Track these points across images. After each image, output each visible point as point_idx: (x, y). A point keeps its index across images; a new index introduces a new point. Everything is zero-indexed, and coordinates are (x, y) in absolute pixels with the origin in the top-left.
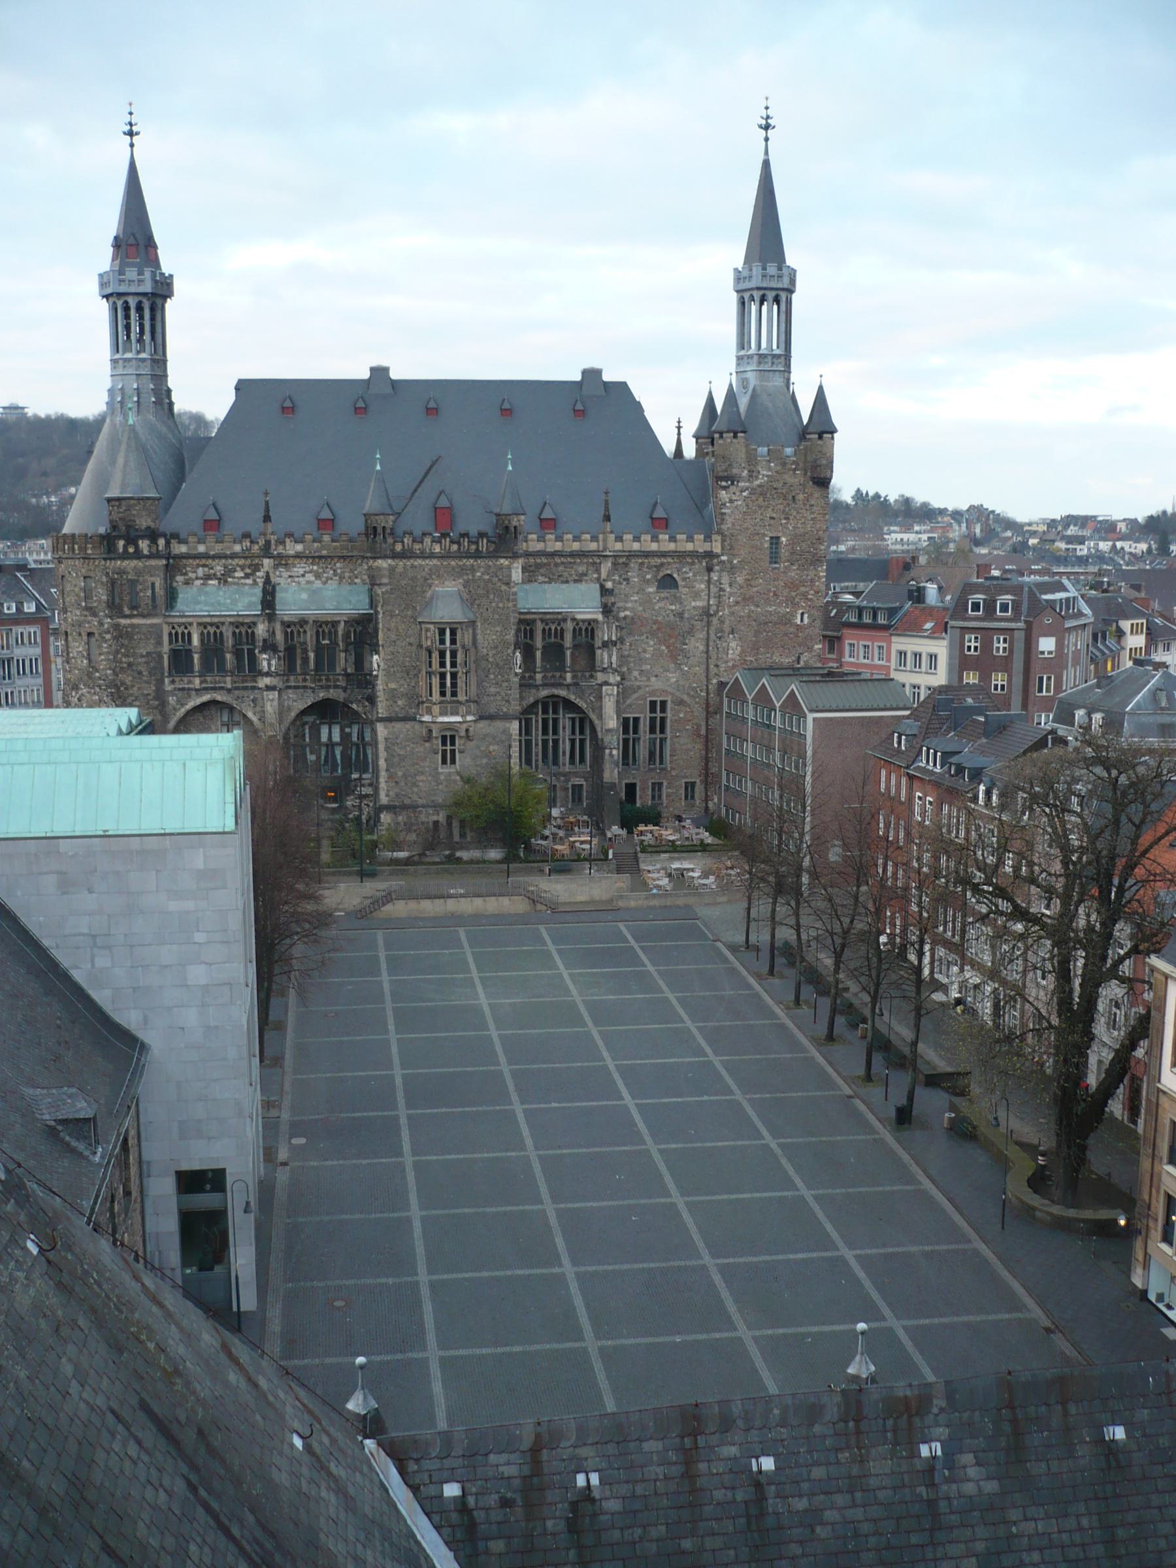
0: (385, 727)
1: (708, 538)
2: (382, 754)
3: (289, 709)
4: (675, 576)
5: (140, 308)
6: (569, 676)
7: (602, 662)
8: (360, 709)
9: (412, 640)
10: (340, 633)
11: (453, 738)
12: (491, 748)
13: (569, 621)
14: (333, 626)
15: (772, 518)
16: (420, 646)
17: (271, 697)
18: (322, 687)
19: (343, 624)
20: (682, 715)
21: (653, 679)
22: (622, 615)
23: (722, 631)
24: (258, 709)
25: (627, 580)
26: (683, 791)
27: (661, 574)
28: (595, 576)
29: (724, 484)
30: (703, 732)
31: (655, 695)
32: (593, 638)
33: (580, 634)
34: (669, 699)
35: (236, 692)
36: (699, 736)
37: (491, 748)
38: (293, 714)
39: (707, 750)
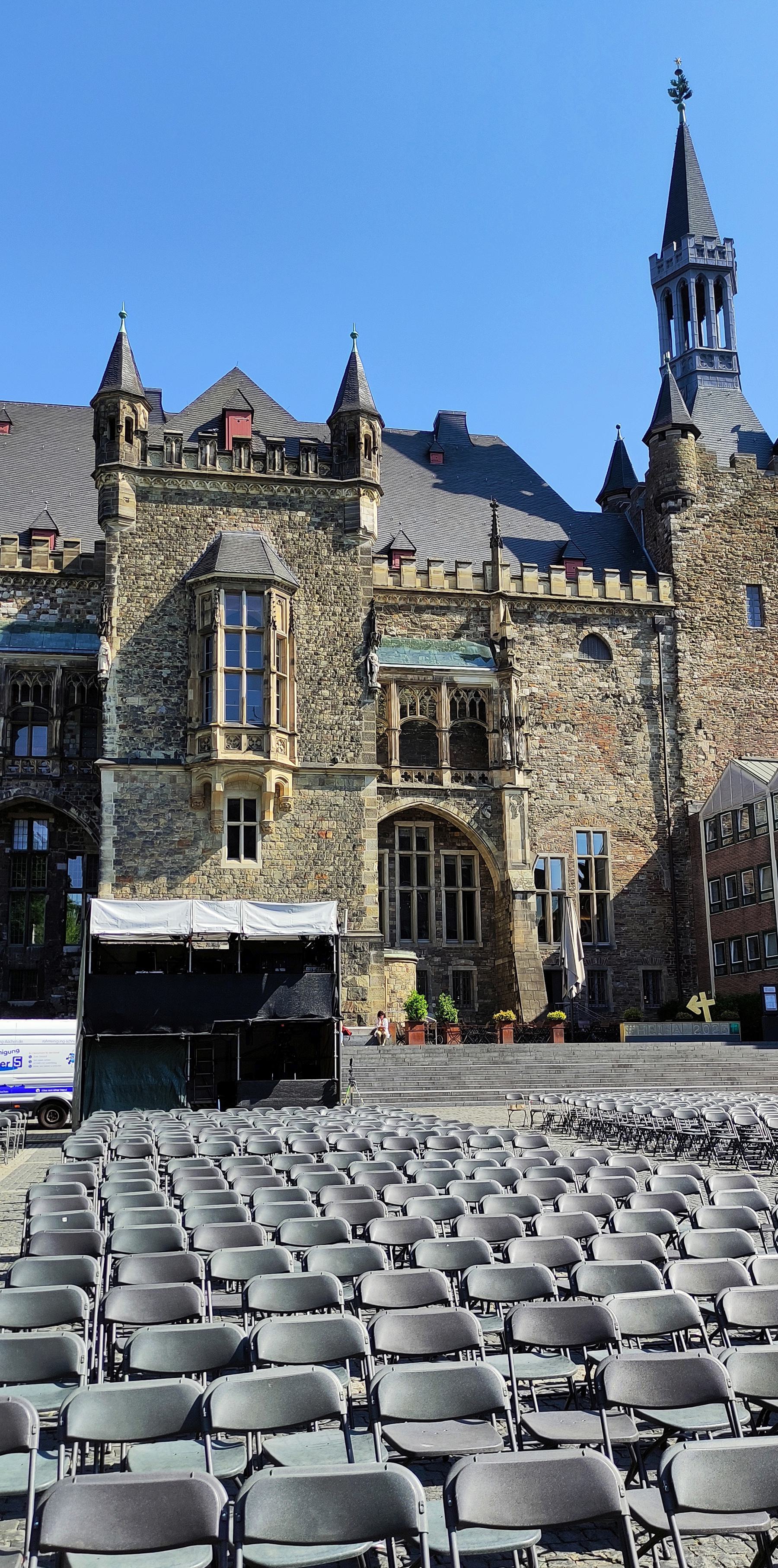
0: (118, 778)
1: (653, 581)
2: (109, 832)
4: (606, 636)
6: (447, 776)
7: (501, 752)
8: (83, 817)
9: (176, 621)
10: (54, 688)
11: (251, 805)
12: (325, 825)
13: (444, 687)
14: (43, 677)
15: (746, 558)
16: (192, 628)
18: (16, 777)
19: (59, 673)
20: (629, 858)
21: (581, 797)
22: (527, 692)
23: (685, 723)
25: (531, 638)
26: (640, 987)
27: (585, 633)
28: (482, 629)
29: (671, 504)
30: (666, 886)
31: (583, 824)
32: (483, 718)
33: (462, 711)
34: (608, 828)
36: (660, 892)
37: (325, 825)
39: (677, 918)
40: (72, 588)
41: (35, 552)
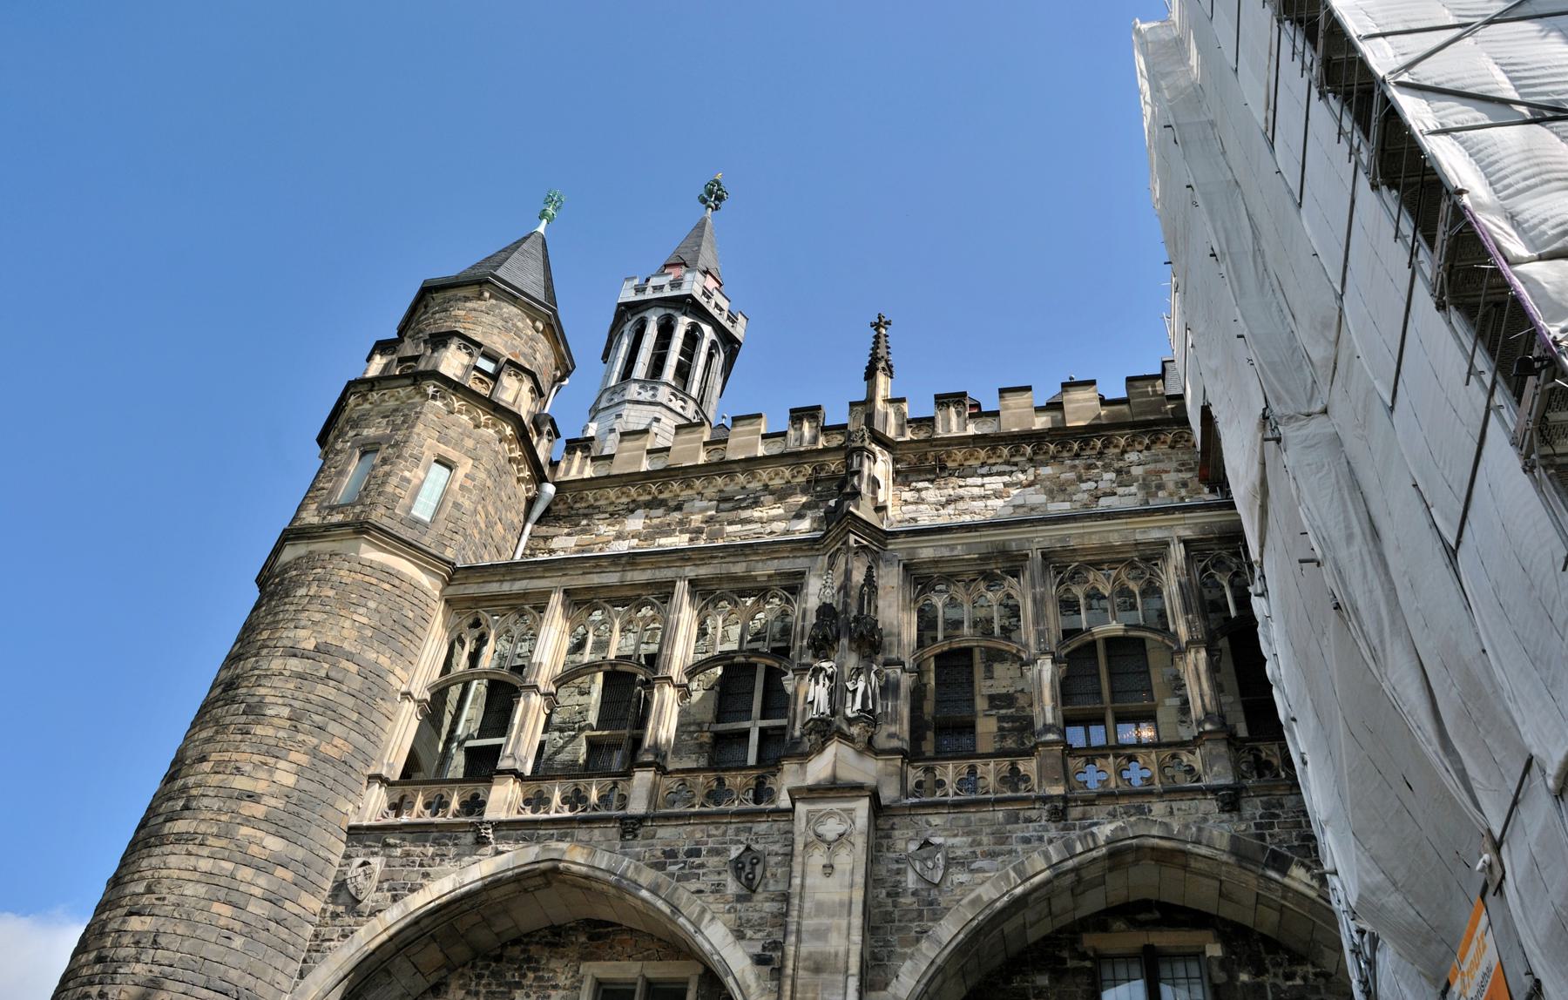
3: (932, 909)
5: (666, 331)
17: (831, 828)
19: (1177, 553)
24: (764, 905)
35: (666, 833)
38: (948, 930)
40: (1160, 449)
41: (1070, 401)
